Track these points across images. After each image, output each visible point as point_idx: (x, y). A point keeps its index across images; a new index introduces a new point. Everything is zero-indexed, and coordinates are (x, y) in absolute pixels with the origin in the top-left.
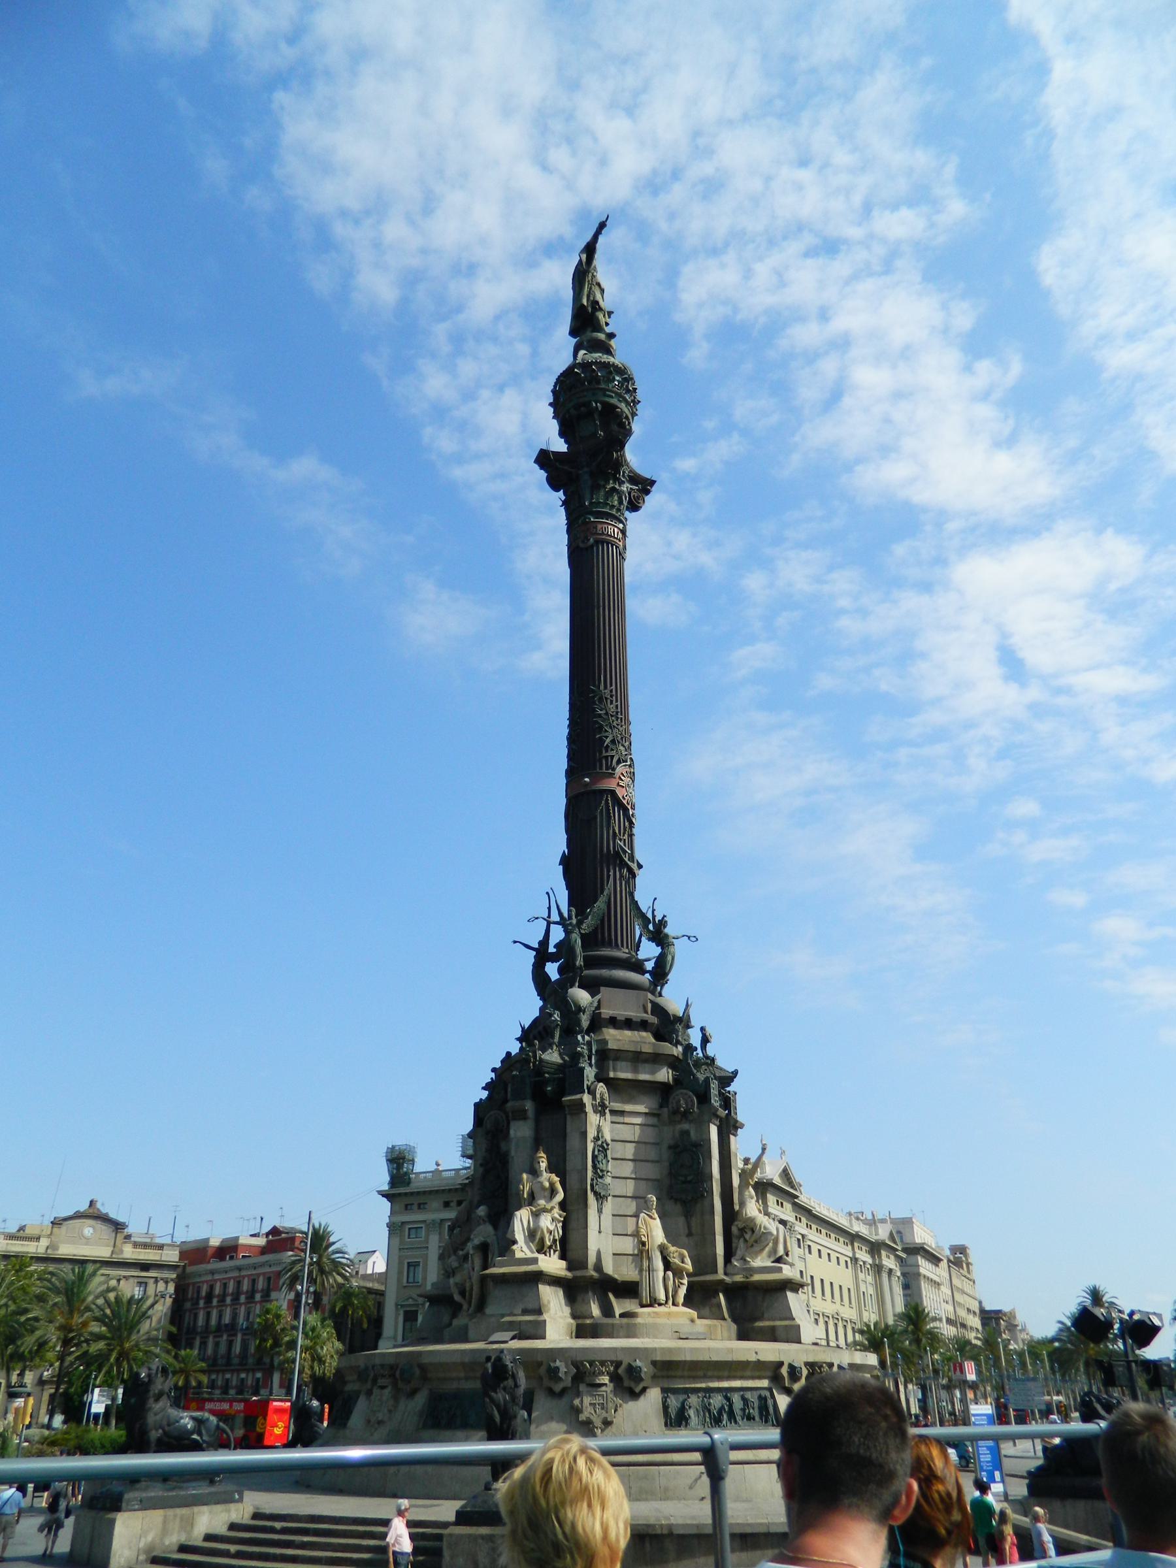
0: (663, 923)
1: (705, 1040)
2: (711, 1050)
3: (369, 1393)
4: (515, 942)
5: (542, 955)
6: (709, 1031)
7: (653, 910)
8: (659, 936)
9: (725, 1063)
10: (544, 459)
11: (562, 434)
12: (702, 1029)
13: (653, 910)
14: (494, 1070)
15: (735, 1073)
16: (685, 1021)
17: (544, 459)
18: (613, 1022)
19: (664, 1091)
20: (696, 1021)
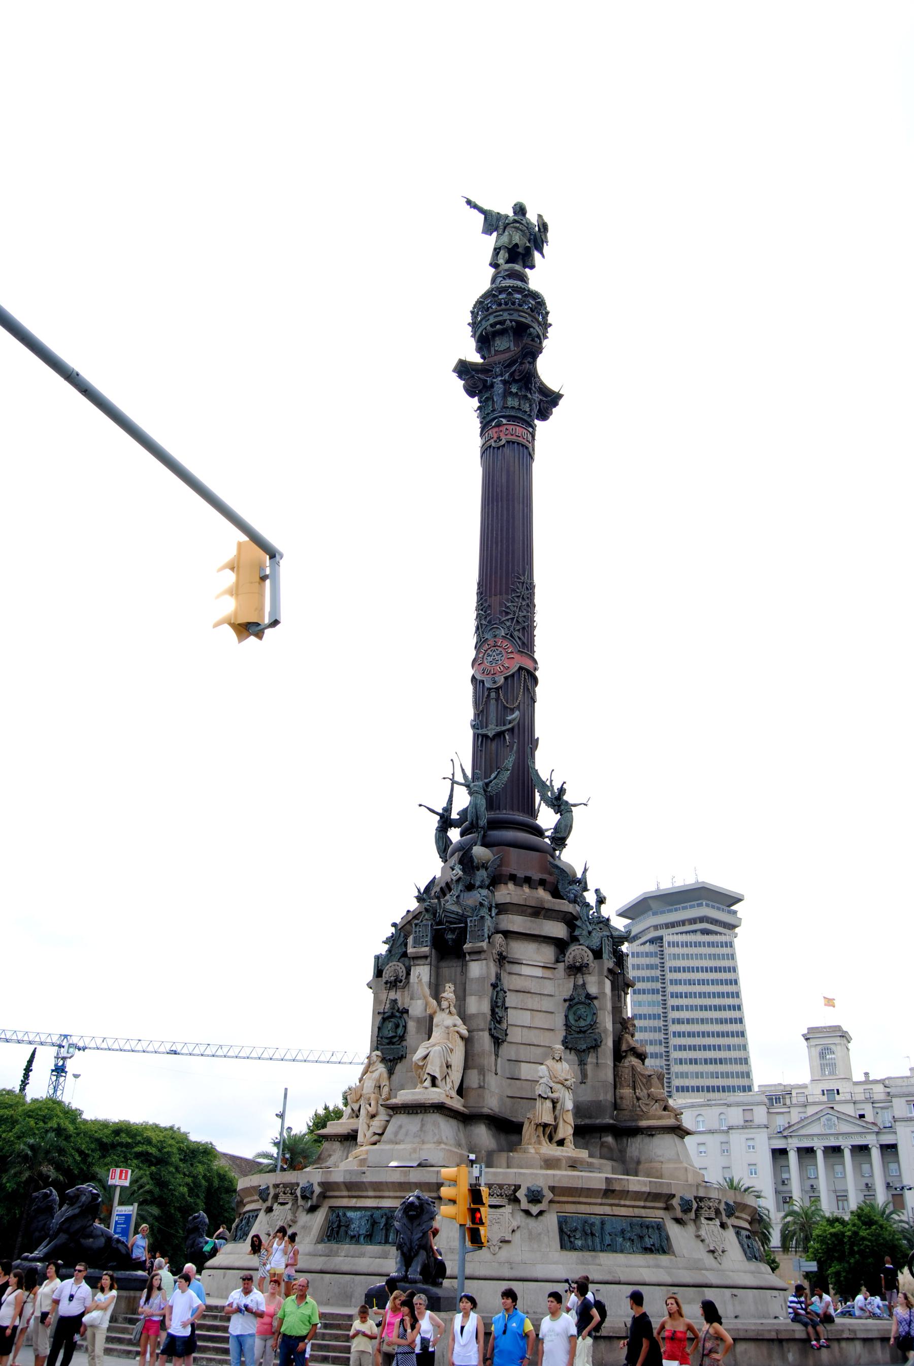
0: (562, 791)
1: (601, 901)
3: (270, 1210)
4: (420, 805)
5: (446, 822)
6: (604, 892)
7: (551, 781)
8: (558, 803)
10: (463, 369)
11: (479, 350)
12: (597, 891)
13: (551, 781)
14: (394, 925)
16: (583, 884)
17: (463, 369)
18: (513, 878)
19: (561, 946)
20: (592, 885)
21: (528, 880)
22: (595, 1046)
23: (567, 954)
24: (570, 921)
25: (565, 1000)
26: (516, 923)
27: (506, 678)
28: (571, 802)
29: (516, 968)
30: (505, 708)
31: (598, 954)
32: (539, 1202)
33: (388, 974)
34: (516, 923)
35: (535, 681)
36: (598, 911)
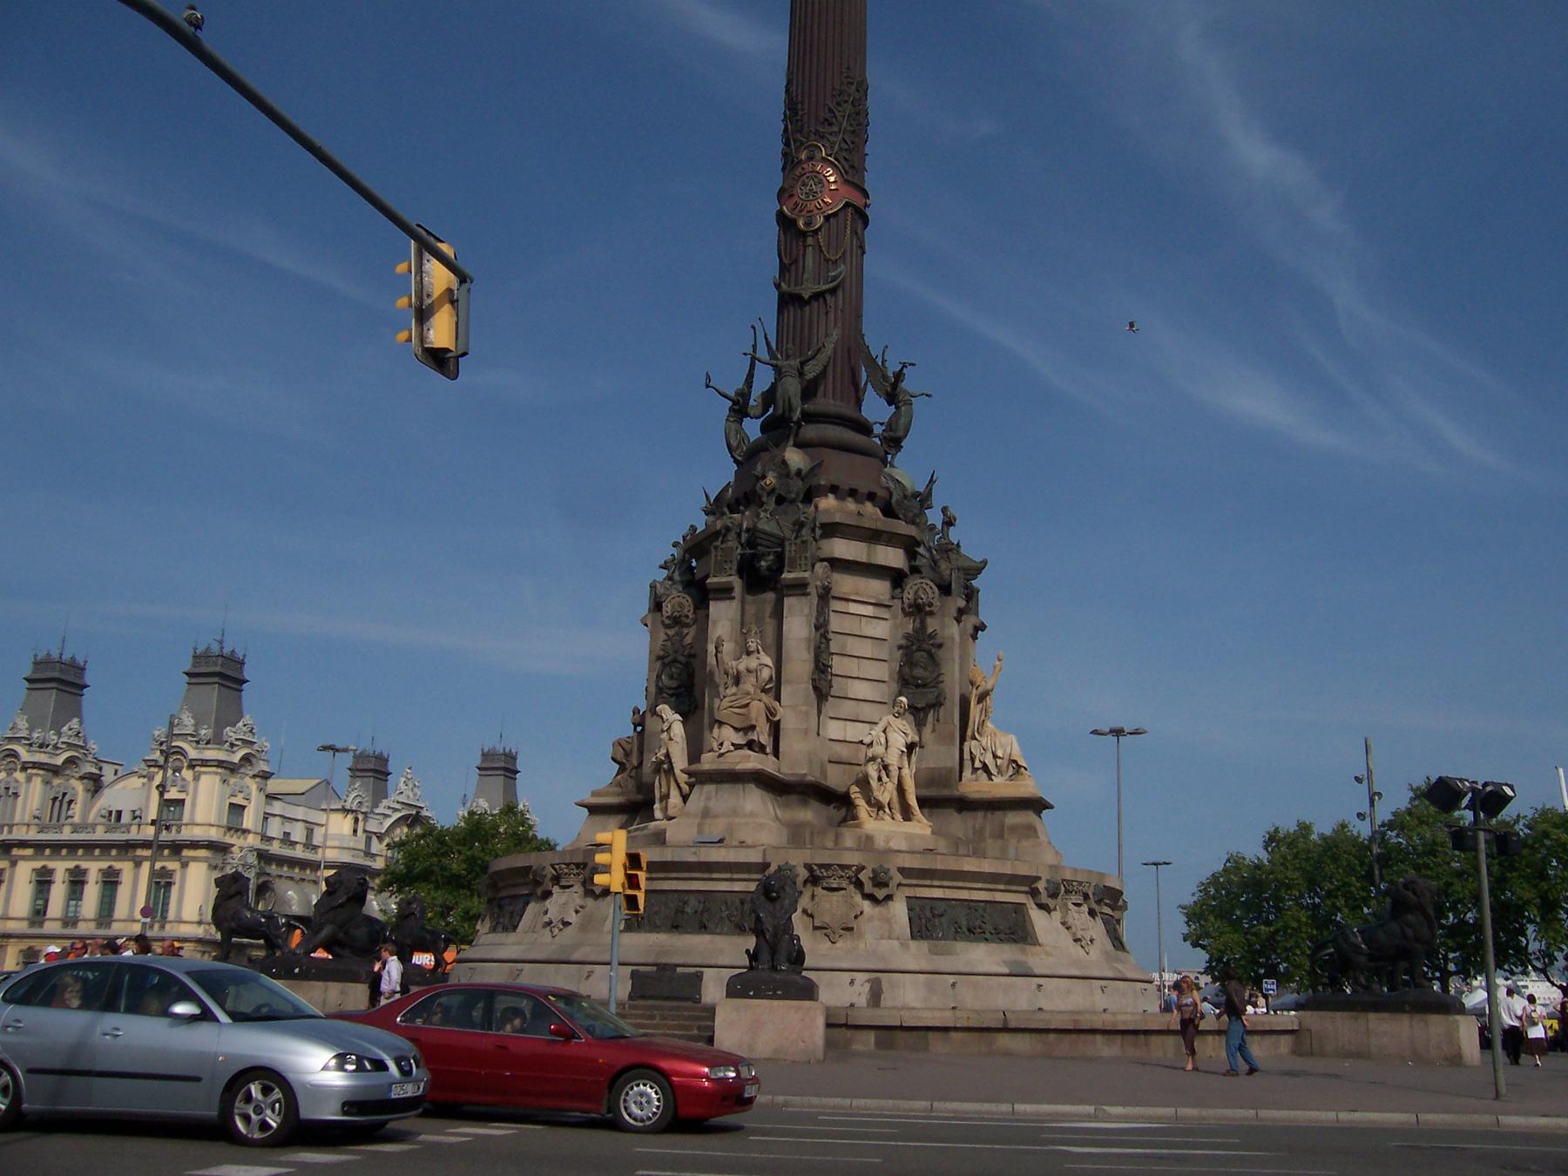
1: (949, 523)
2: (954, 535)
6: (952, 511)
7: (884, 361)
9: (972, 551)
12: (944, 510)
13: (884, 361)
15: (985, 563)
19: (897, 578)
21: (853, 493)
22: (937, 704)
23: (907, 588)
24: (910, 547)
25: (900, 647)
26: (842, 548)
27: (827, 218)
28: (911, 390)
29: (836, 605)
30: (827, 261)
31: (945, 589)
32: (886, 885)
33: (668, 608)
34: (842, 548)
35: (866, 221)
36: (945, 534)
